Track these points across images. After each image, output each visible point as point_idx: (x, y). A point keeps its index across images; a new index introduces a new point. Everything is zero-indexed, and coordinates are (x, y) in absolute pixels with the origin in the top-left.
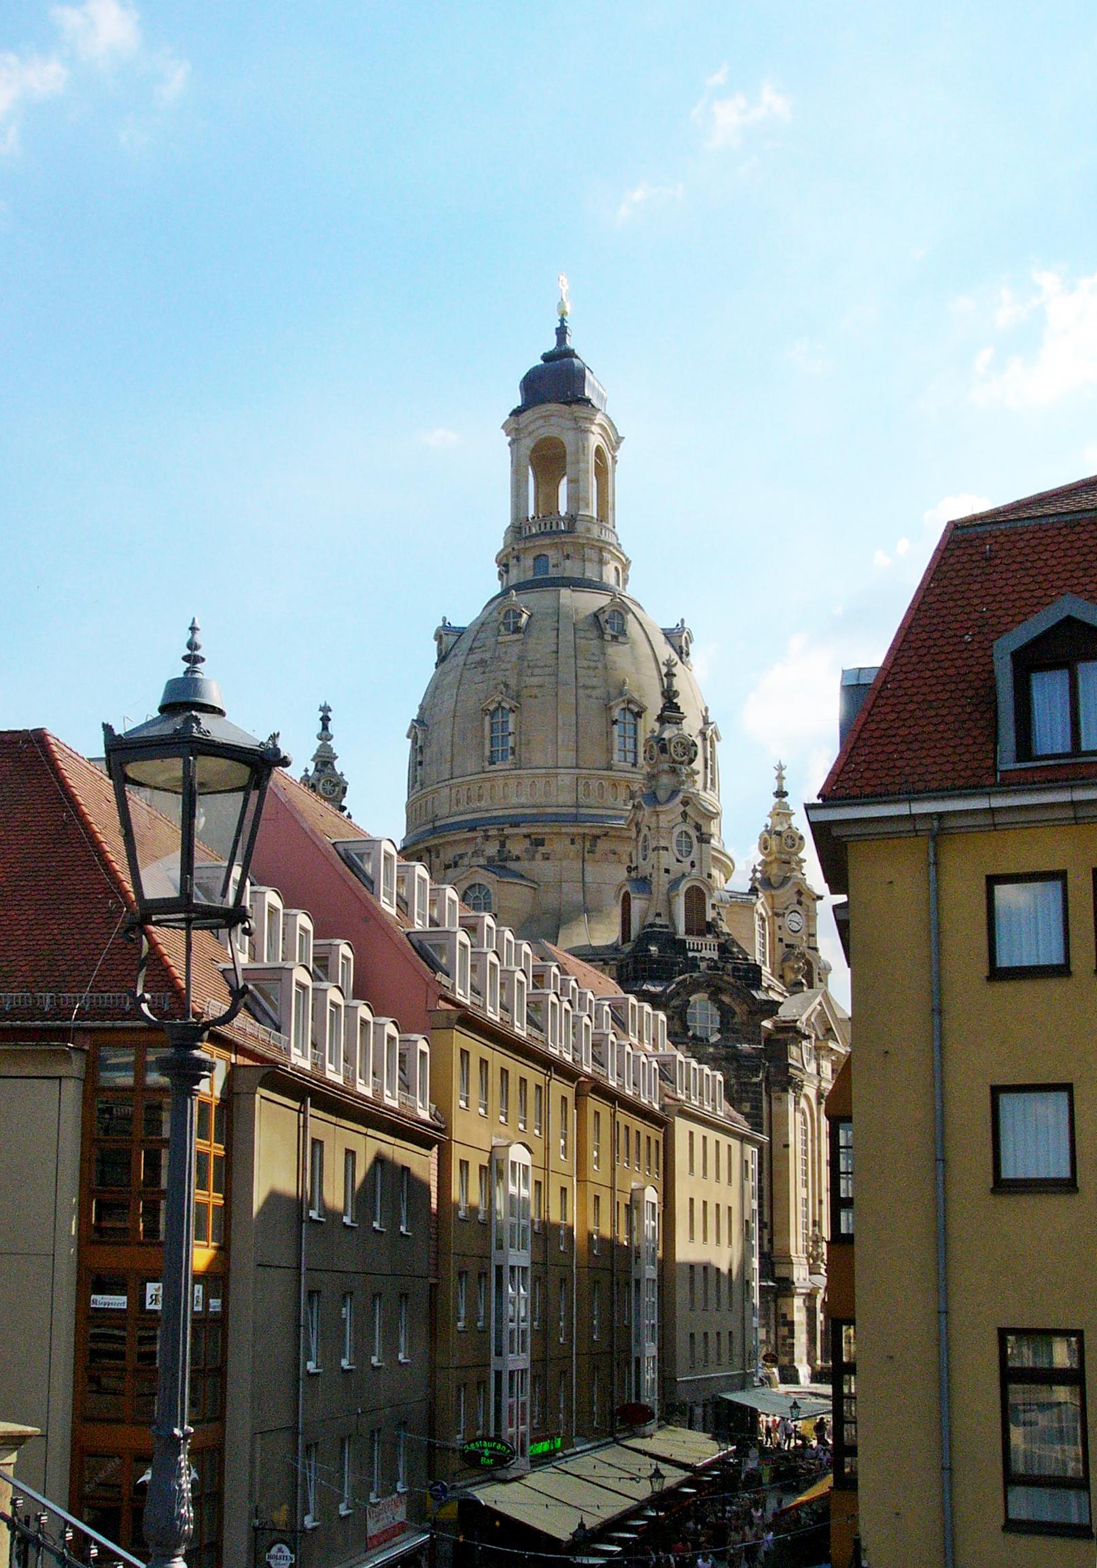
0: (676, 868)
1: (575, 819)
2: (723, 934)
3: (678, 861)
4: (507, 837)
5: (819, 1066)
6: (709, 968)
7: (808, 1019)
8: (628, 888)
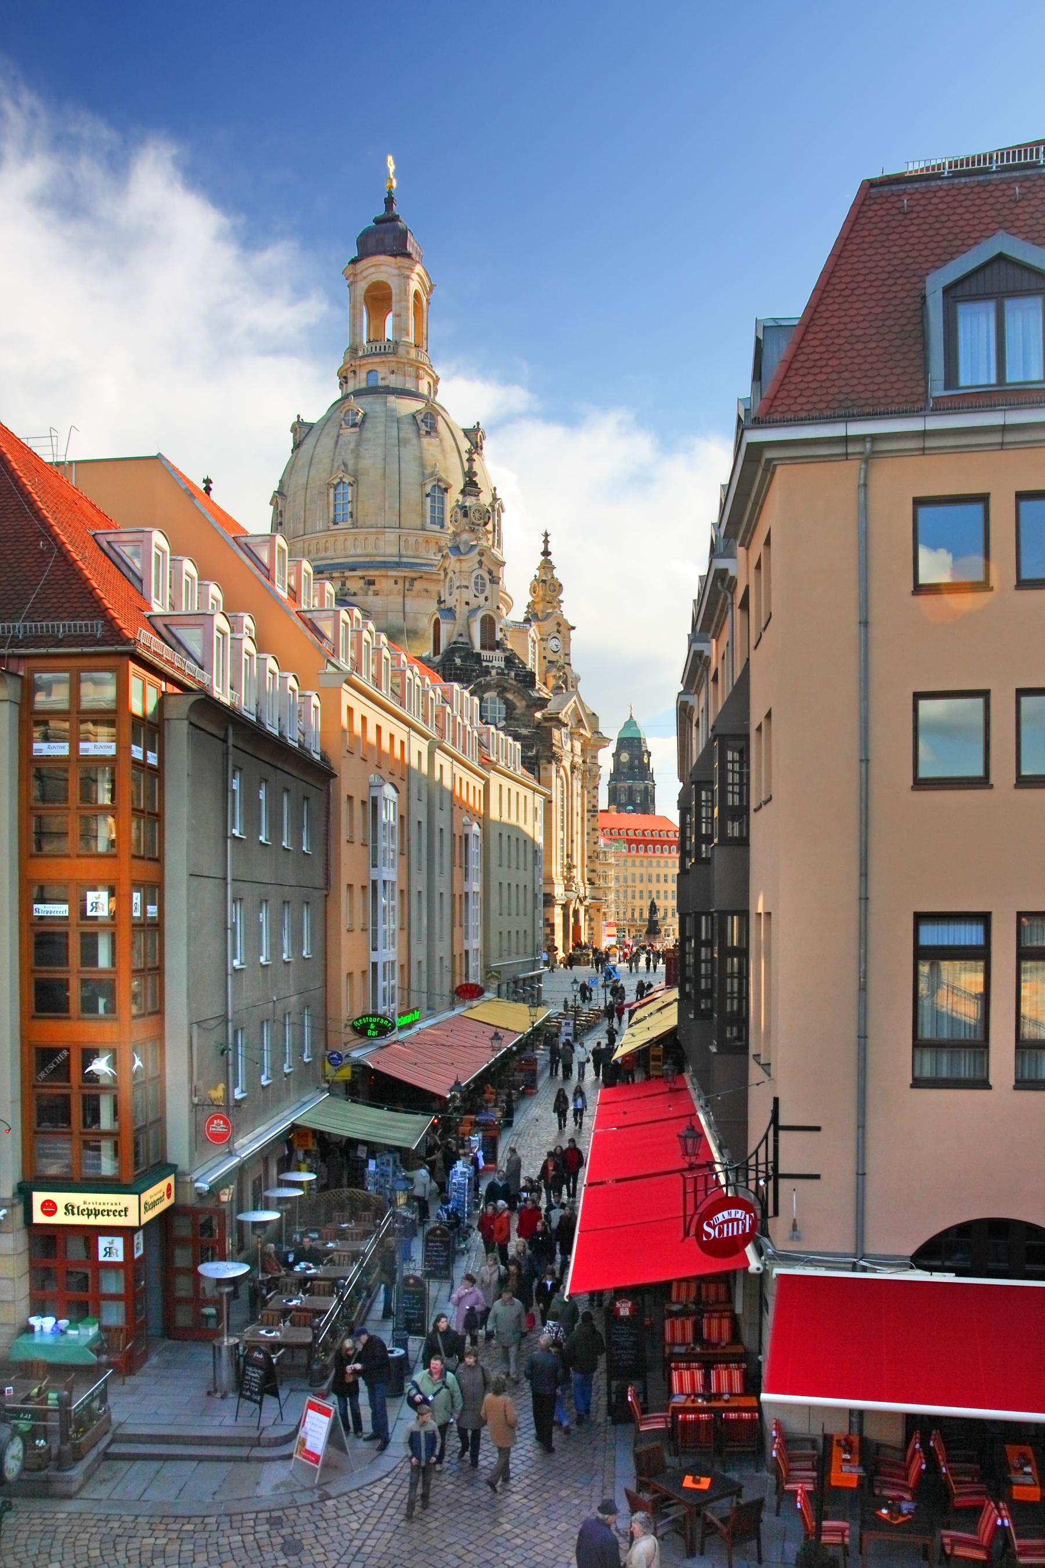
0: (474, 603)
1: (398, 565)
2: (508, 649)
4: (347, 578)
5: (572, 746)
6: (498, 674)
8: (438, 616)
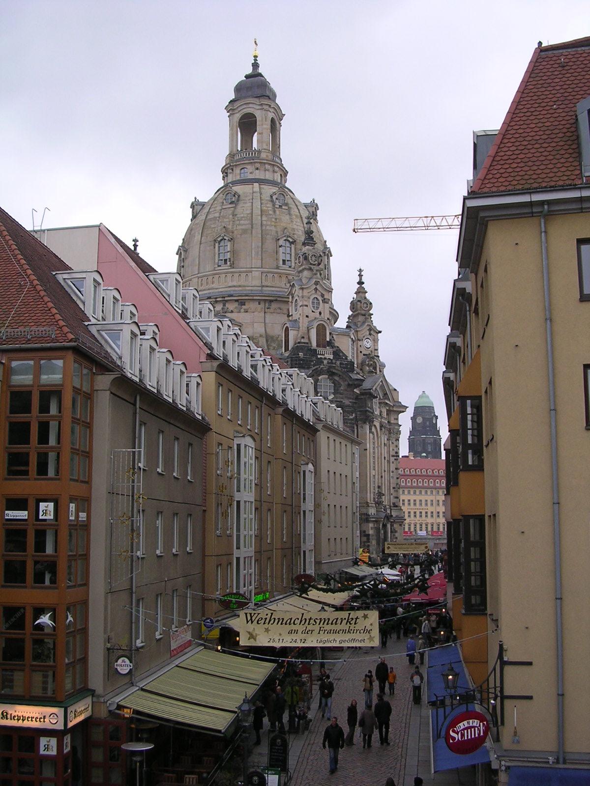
0: (312, 316)
2: (335, 347)
3: (313, 312)
5: (381, 412)
6: (328, 363)
7: (376, 389)
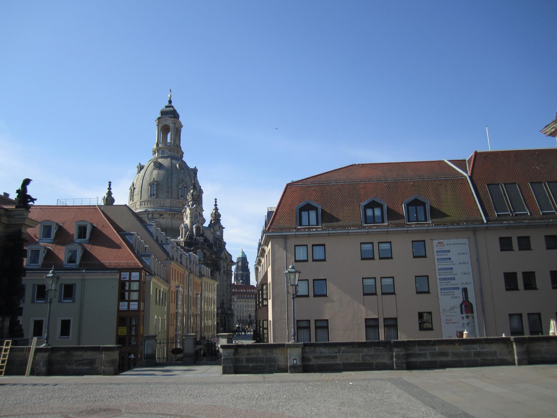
0: (194, 222)
